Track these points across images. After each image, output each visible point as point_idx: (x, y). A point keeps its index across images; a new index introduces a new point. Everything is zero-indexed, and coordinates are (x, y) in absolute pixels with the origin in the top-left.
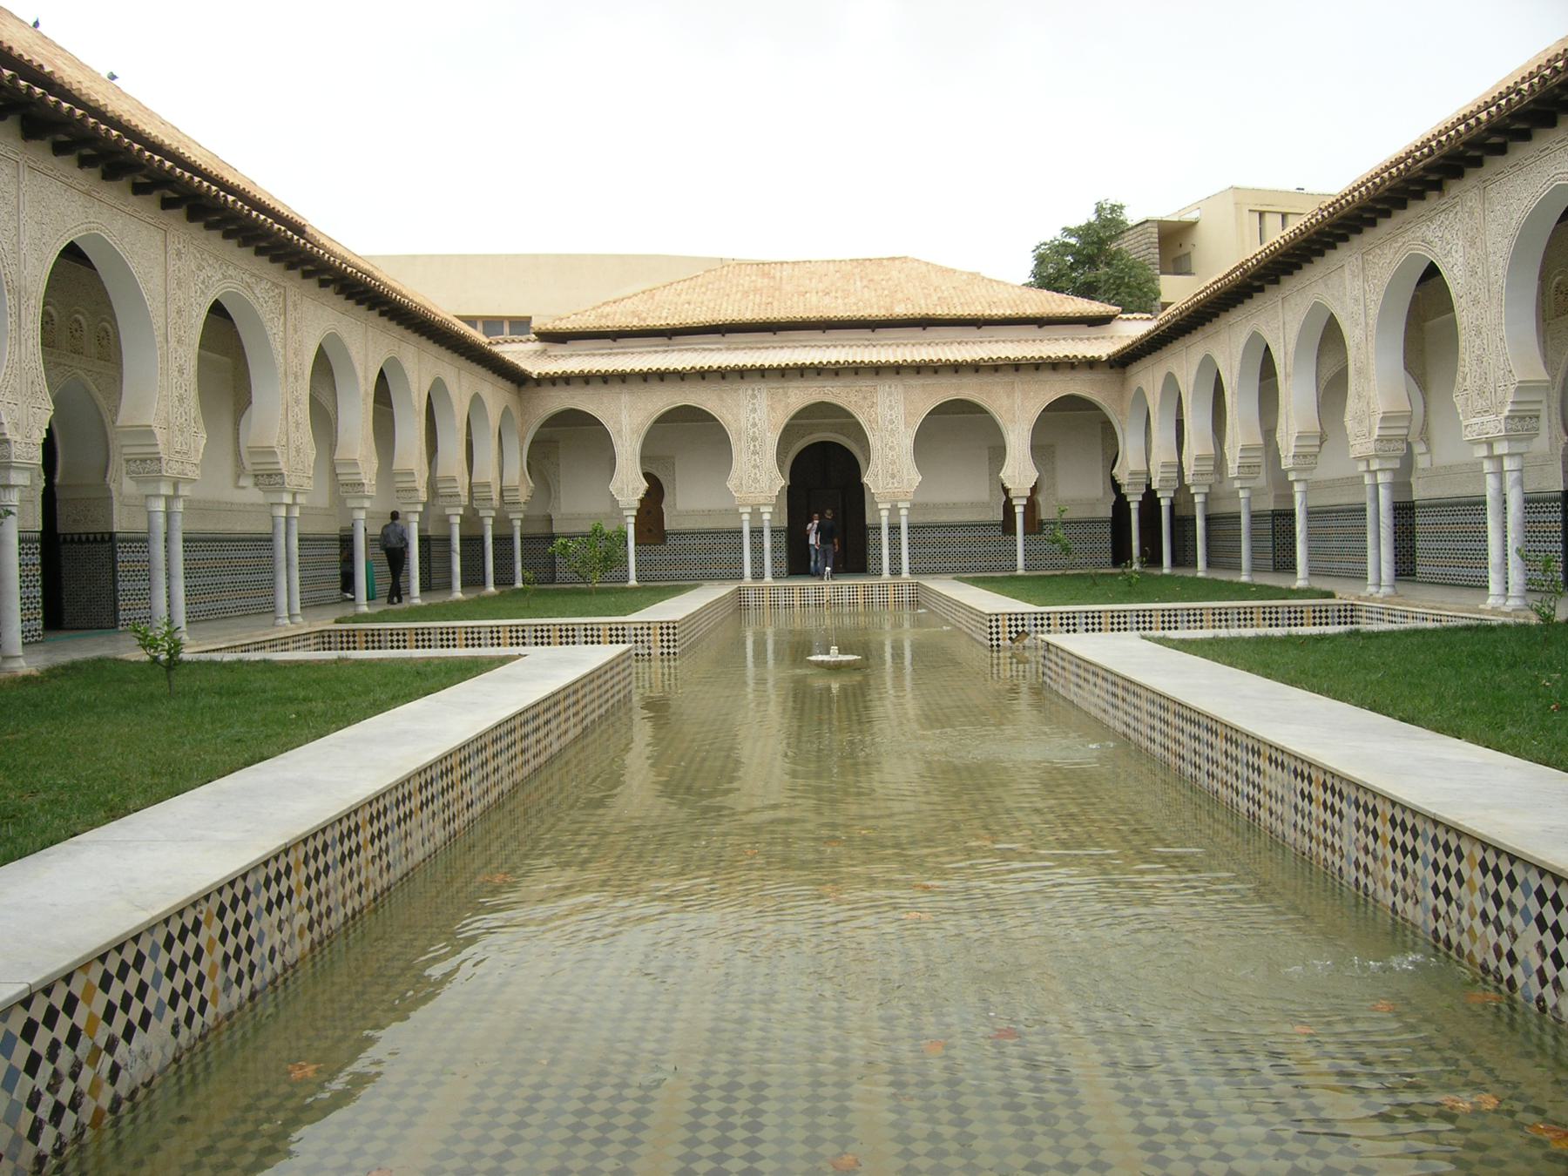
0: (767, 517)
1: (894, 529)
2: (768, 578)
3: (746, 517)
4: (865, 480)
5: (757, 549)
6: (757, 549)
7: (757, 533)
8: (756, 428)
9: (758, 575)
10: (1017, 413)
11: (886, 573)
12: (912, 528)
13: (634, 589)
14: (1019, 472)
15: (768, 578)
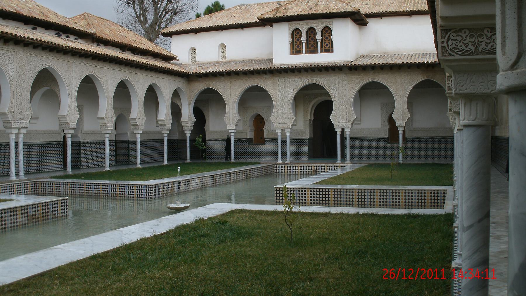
0: (288, 134)
1: (343, 140)
2: (288, 161)
3: (279, 134)
4: (331, 117)
5: (284, 147)
6: (284, 147)
7: (284, 140)
8: (283, 94)
9: (284, 159)
10: (400, 88)
11: (339, 161)
12: (351, 139)
13: (233, 163)
14: (401, 115)
15: (288, 161)
